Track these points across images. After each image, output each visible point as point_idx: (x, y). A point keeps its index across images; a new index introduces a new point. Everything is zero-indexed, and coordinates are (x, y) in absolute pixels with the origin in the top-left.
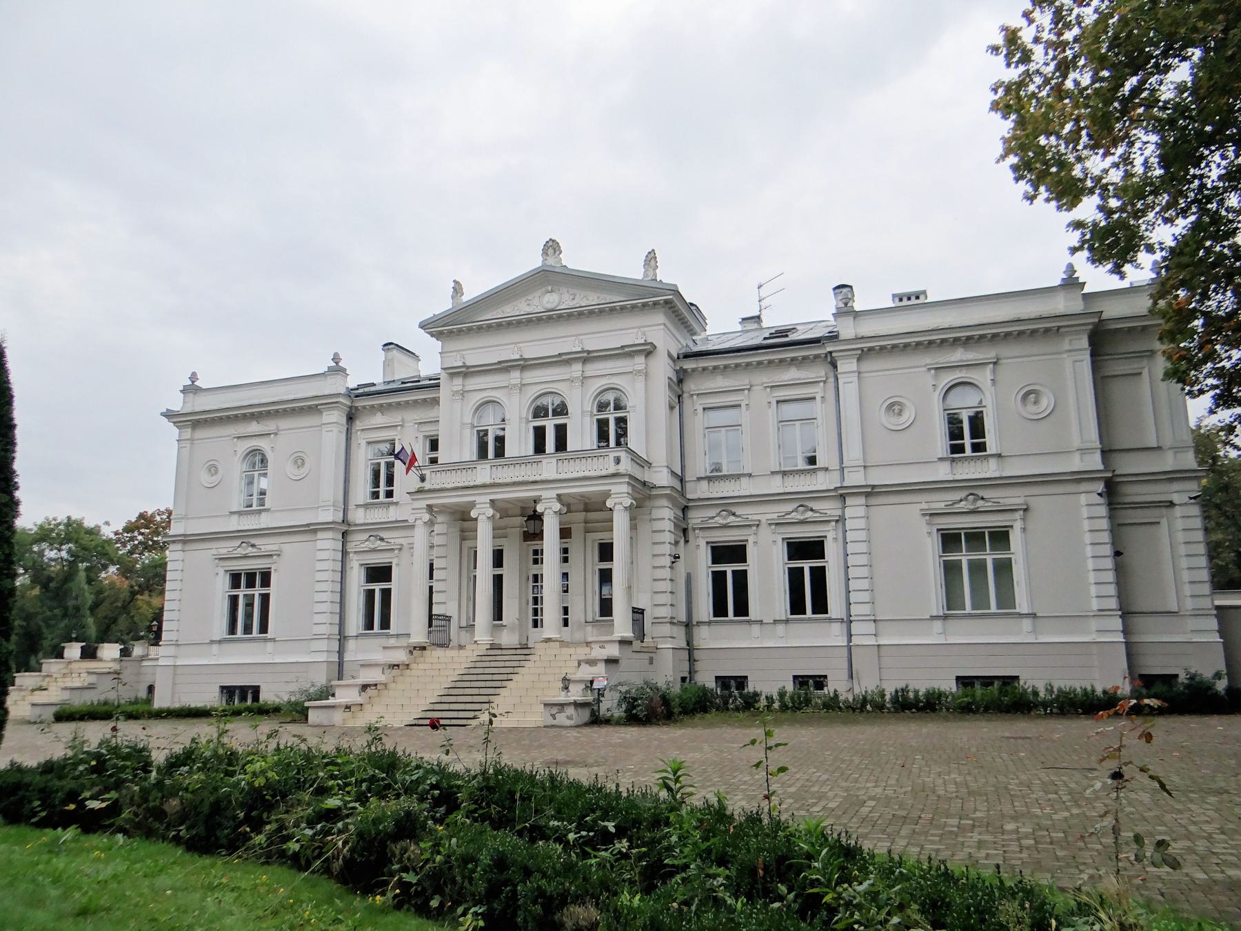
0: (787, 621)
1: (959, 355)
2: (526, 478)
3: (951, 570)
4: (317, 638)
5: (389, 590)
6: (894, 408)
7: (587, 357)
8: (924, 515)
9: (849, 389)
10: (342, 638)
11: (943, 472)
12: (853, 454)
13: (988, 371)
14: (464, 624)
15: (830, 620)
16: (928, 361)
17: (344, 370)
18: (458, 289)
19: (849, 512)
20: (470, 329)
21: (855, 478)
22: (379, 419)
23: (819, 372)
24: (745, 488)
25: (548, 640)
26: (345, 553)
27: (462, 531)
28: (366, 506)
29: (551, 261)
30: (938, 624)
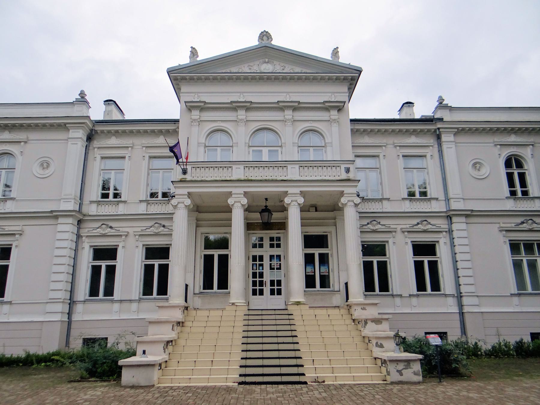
0: (418, 296)
1: (513, 139)
2: (274, 178)
3: (517, 265)
4: (53, 301)
5: (114, 267)
6: (477, 165)
7: (297, 107)
8: (501, 231)
9: (449, 151)
10: (72, 303)
11: (510, 205)
12: (454, 190)
13: (529, 150)
14: (197, 291)
15: (446, 295)
16: (496, 140)
17: (87, 102)
18: (194, 52)
19: (455, 227)
20: (207, 79)
21: (454, 205)
22: (113, 141)
23: (431, 141)
24: (387, 207)
25: (298, 303)
26: (79, 236)
27: (197, 220)
28: (98, 203)
29: (265, 42)
30: (516, 300)
